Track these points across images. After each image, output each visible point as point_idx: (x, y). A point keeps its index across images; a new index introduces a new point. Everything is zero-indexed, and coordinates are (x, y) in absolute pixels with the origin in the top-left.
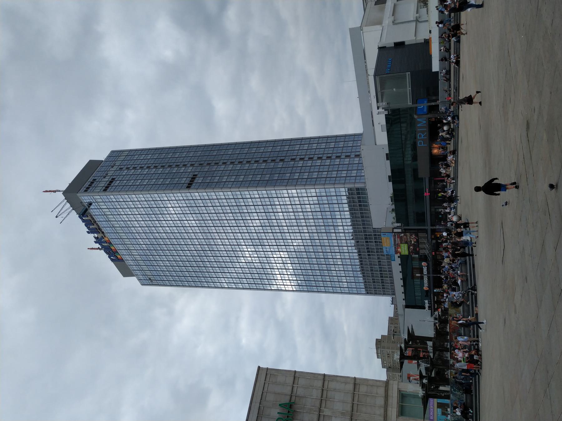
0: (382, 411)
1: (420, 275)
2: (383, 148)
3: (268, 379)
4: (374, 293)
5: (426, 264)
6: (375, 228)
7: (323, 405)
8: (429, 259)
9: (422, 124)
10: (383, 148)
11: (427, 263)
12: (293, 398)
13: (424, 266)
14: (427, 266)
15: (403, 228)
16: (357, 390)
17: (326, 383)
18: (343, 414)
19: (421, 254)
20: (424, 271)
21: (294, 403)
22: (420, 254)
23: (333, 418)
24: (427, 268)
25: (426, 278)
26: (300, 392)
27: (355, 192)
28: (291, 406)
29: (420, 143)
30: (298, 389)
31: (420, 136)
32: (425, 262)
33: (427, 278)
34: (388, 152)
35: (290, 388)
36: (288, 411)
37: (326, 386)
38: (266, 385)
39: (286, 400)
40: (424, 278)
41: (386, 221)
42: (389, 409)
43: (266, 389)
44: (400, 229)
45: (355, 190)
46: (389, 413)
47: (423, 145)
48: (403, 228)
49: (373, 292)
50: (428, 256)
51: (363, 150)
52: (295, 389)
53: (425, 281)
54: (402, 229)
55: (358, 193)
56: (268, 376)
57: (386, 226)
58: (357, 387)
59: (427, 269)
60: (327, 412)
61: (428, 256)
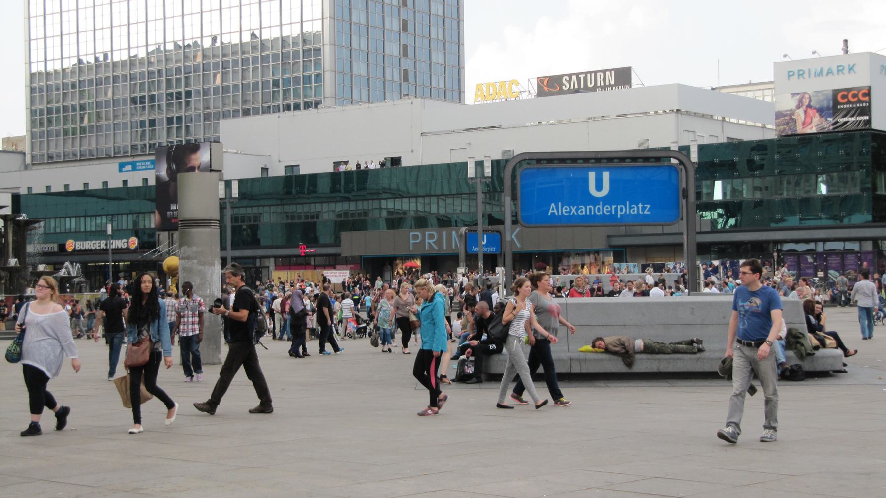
1: (109, 232)
2: (413, 151)
4: (33, 108)
5: (133, 247)
6: (217, 125)
8: (147, 252)
9: (456, 243)
10: (413, 151)
11: (136, 249)
13: (127, 242)
14: (129, 249)
15: (227, 201)
19: (159, 235)
20: (116, 241)
22: (157, 233)
24: (125, 249)
25: (98, 245)
27: (312, 72)
29: (416, 237)
31: (431, 236)
32: (139, 244)
33: (98, 248)
34: (404, 163)
40: (96, 240)
41: (237, 153)
44: (226, 196)
45: (317, 72)
47: (411, 241)
48: (227, 201)
49: (37, 107)
50: (155, 252)
51: (412, 103)
53: (89, 242)
54: (225, 198)
55: (307, 79)
57: (225, 154)
59: (121, 249)
61: (155, 252)
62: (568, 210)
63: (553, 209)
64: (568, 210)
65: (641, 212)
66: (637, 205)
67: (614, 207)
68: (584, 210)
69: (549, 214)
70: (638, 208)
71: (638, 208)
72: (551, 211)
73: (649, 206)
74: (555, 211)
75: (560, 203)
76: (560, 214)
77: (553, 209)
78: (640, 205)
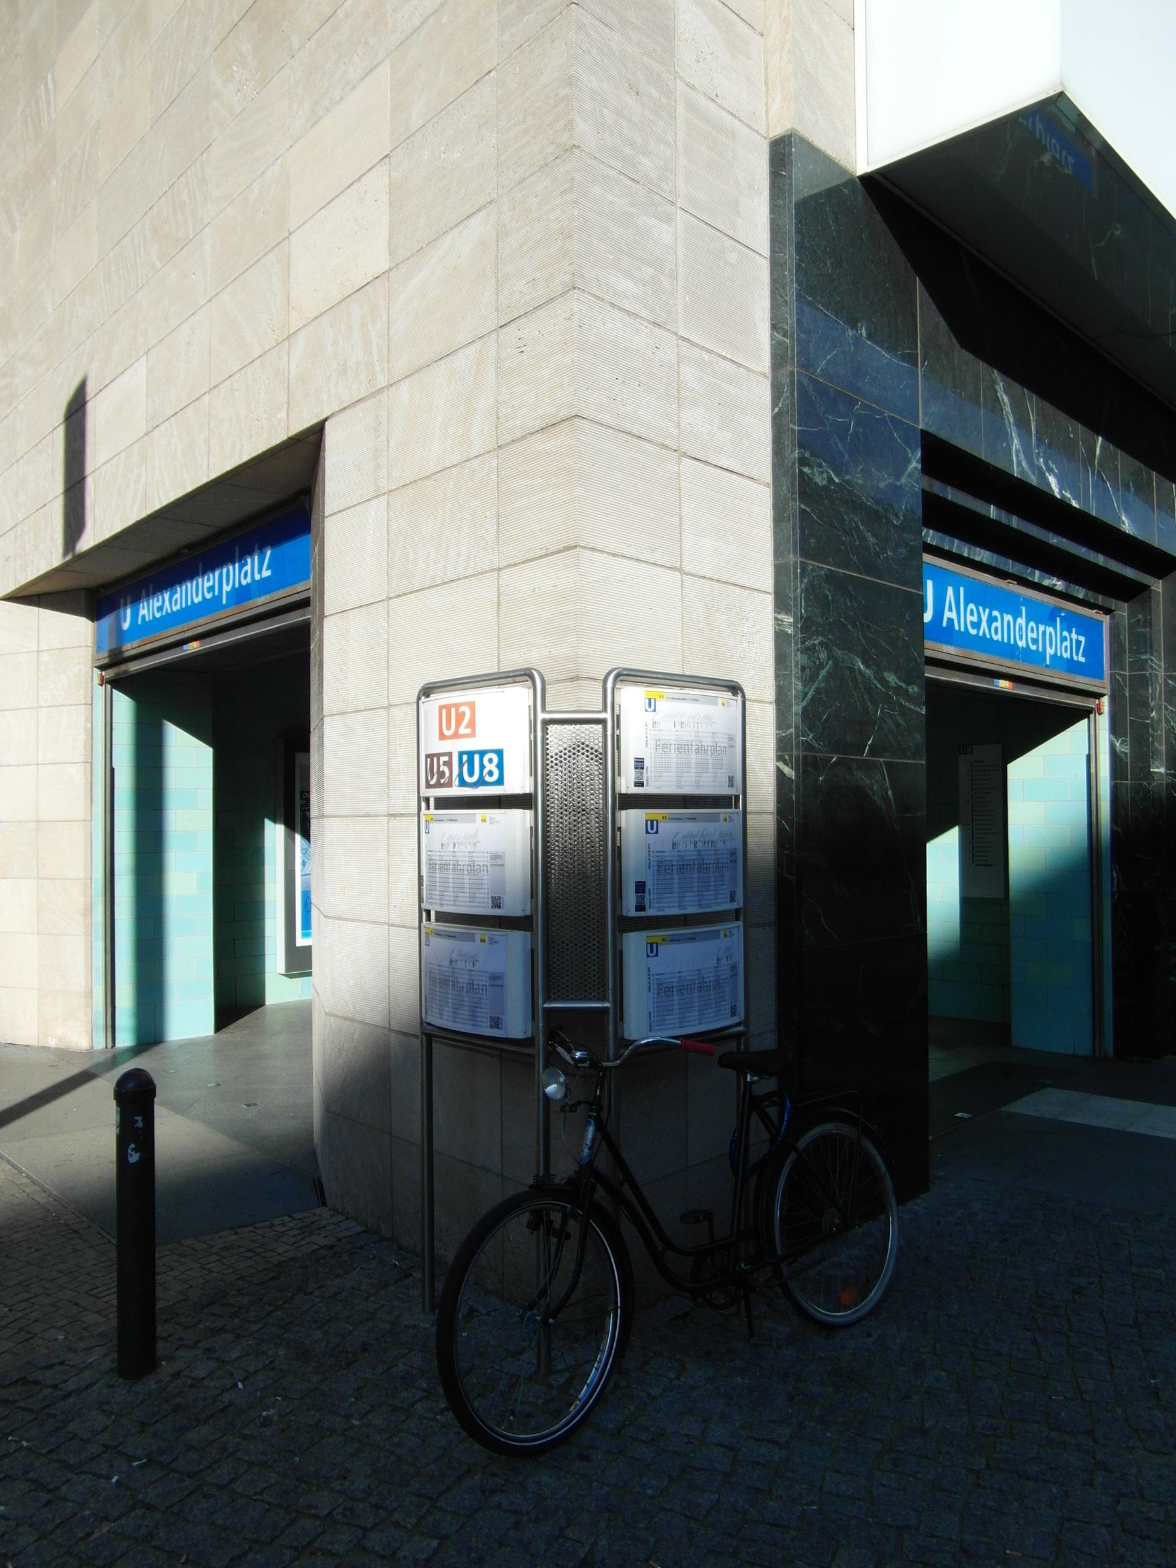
62: (975, 619)
63: (950, 610)
64: (975, 619)
65: (1075, 658)
66: (1070, 632)
67: (1042, 628)
68: (998, 624)
69: (944, 624)
70: (1071, 639)
71: (1071, 639)
72: (947, 614)
73: (1082, 639)
74: (953, 615)
75: (962, 589)
76: (962, 629)
77: (950, 610)
78: (1074, 636)
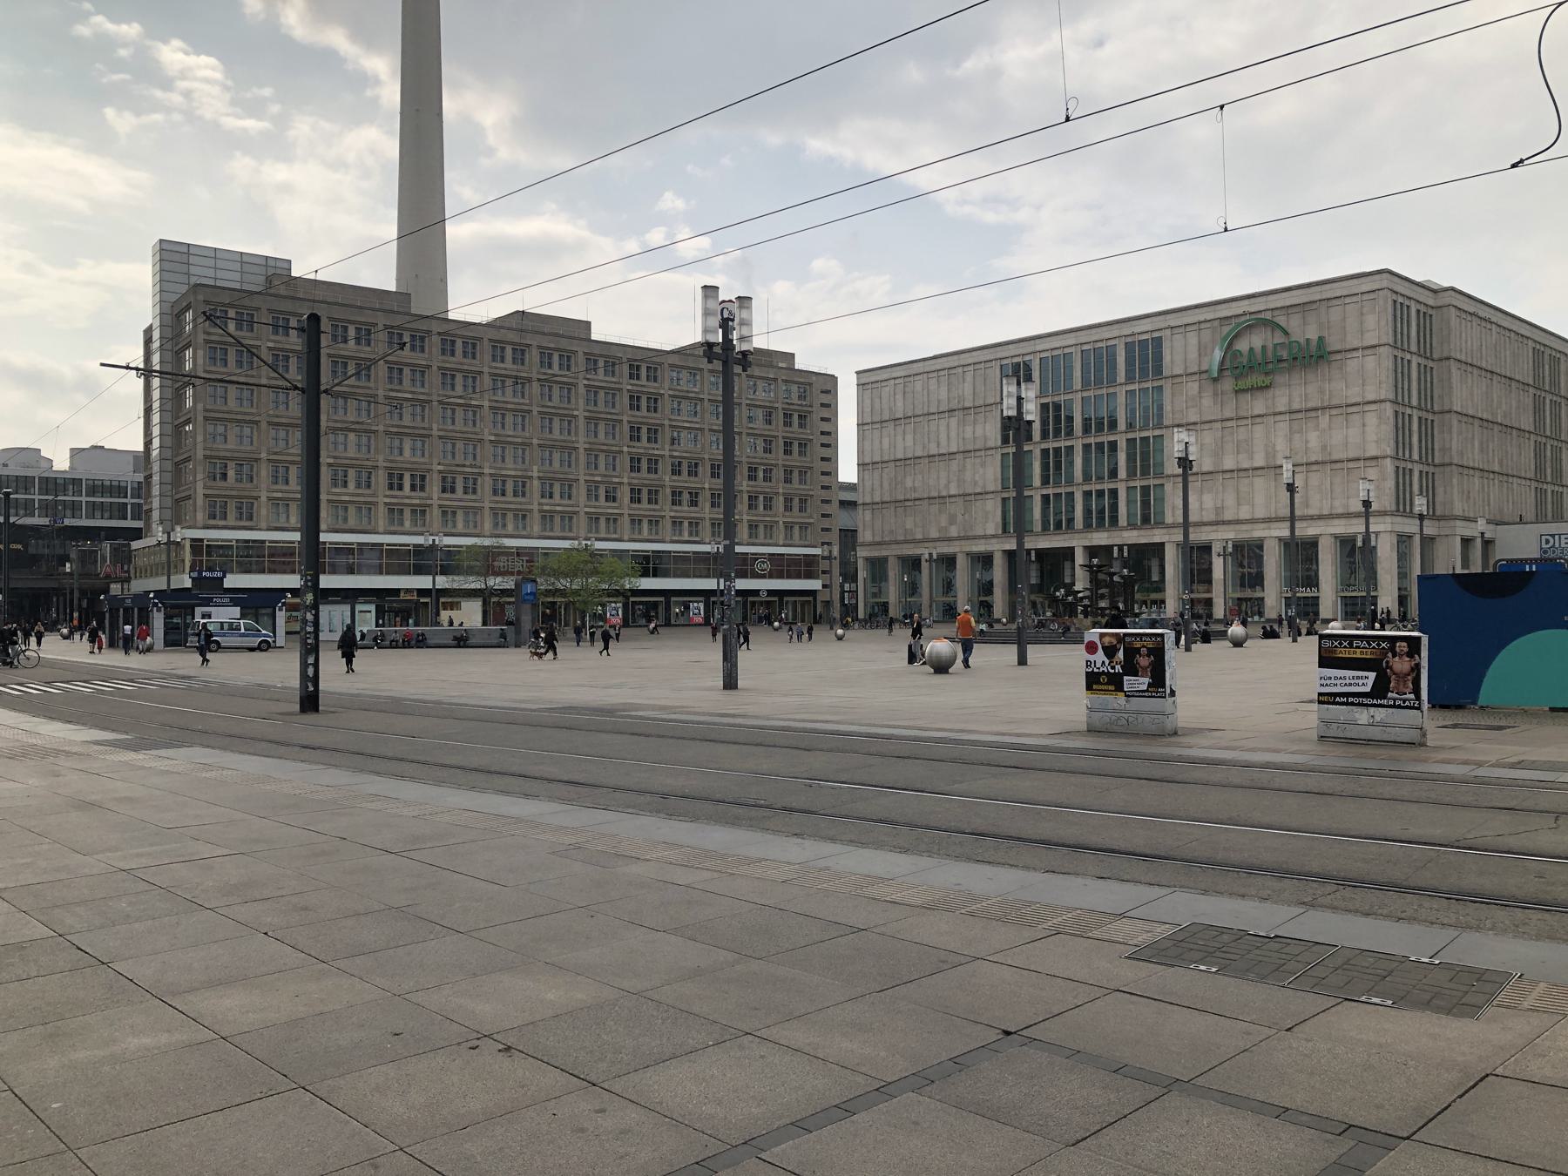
0: (1340, 511)
3: (1366, 297)
7: (1334, 412)
12: (1338, 356)
16: (1368, 463)
17: (1373, 407)
18: (1324, 448)
21: (1329, 362)
23: (1317, 433)
26: (1352, 365)
28: (1322, 357)
30: (1356, 359)
35: (1356, 344)
36: (1312, 356)
37: (1367, 408)
38: (1354, 299)
39: (1334, 343)
42: (1343, 521)
43: (1348, 300)
46: (1336, 522)
52: (1355, 354)
56: (1372, 296)
58: (1373, 463)
60: (1324, 420)
